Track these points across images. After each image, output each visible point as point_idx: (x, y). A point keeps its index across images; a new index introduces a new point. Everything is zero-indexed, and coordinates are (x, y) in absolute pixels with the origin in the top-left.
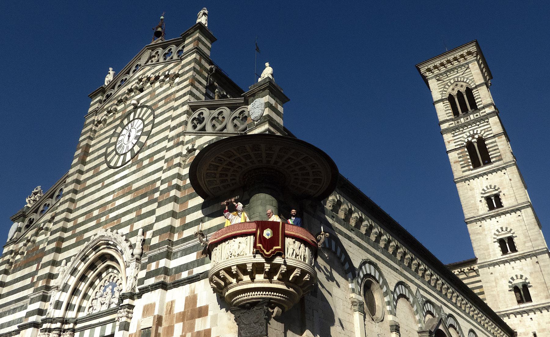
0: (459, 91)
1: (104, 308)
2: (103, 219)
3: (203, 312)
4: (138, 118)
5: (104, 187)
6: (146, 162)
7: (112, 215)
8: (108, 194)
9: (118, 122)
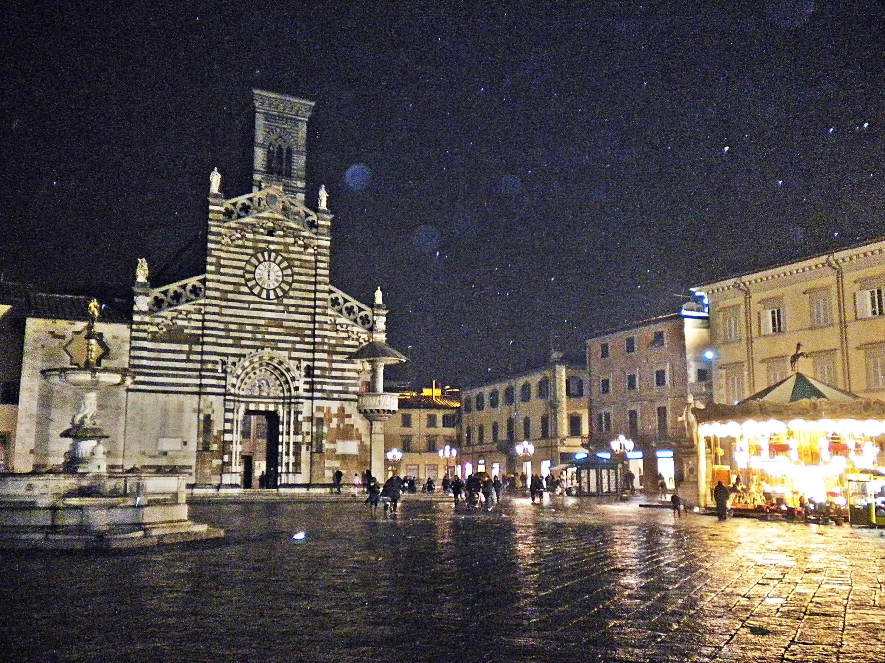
0: (280, 146)
1: (264, 394)
2: (259, 336)
3: (349, 416)
4: (274, 262)
6: (292, 309)
7: (267, 337)
8: (259, 318)
9: (251, 252)
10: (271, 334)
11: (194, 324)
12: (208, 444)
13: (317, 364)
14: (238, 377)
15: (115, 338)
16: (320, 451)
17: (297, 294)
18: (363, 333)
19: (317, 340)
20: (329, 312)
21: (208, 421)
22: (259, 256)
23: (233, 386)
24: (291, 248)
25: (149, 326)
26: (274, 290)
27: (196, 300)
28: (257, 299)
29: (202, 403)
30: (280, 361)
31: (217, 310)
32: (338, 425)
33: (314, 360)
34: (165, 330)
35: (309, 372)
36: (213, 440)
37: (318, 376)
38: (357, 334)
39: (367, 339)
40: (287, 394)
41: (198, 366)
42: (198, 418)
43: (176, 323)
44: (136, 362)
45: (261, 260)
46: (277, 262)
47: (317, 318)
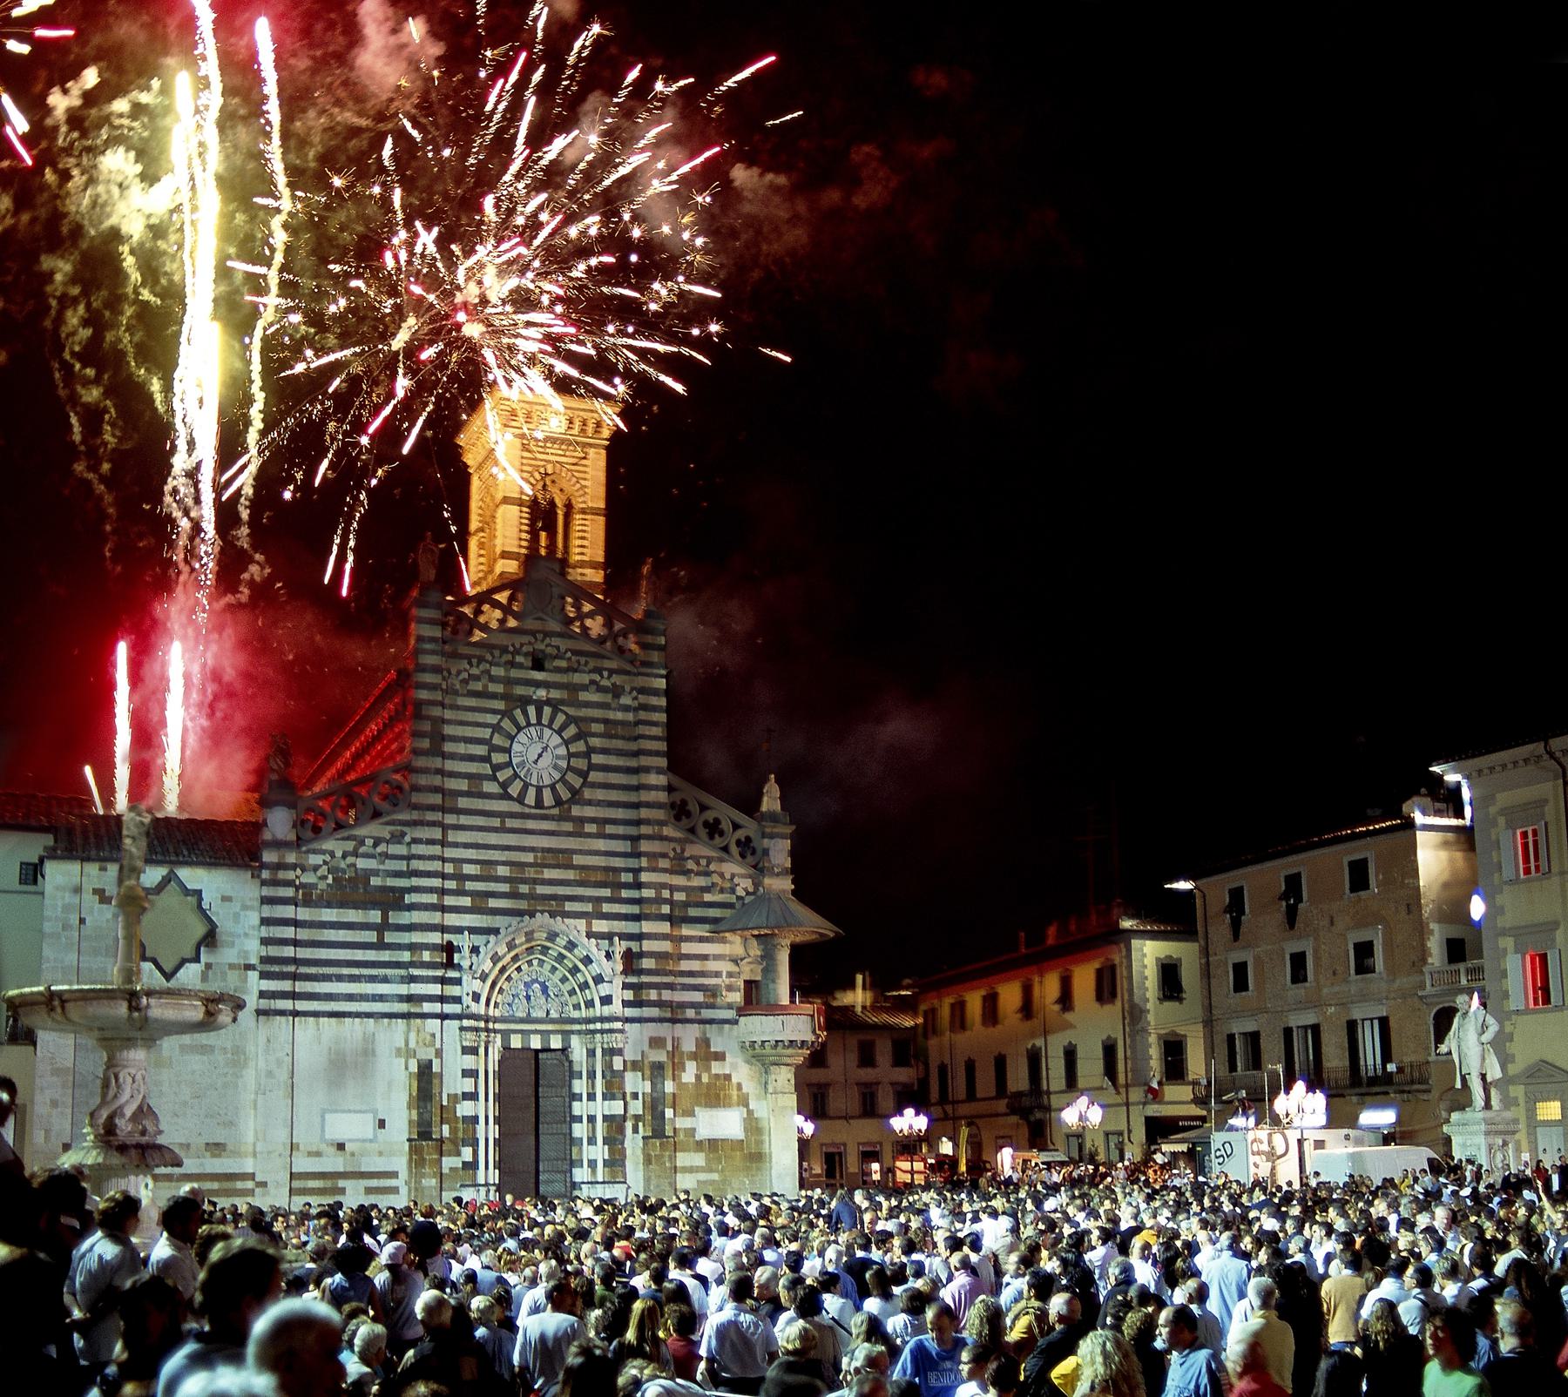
1: (541, 1014)
2: (524, 889)
4: (550, 726)
5: (502, 829)
7: (541, 890)
9: (500, 705)
10: (551, 882)
11: (391, 865)
12: (430, 1125)
13: (647, 945)
14: (484, 977)
15: (226, 899)
16: (658, 1133)
17: (600, 794)
18: (743, 876)
19: (647, 893)
20: (667, 831)
21: (426, 1078)
22: (518, 713)
23: (476, 997)
24: (584, 696)
25: (299, 871)
26: (553, 787)
27: (394, 812)
28: (516, 807)
29: (413, 1036)
30: (570, 942)
31: (437, 833)
32: (698, 1077)
33: (639, 937)
34: (330, 881)
35: (630, 959)
36: (436, 1119)
37: (649, 972)
38: (732, 879)
39: (751, 890)
40: (584, 1013)
41: (406, 956)
42: (407, 1068)
43: (354, 865)
44: (274, 951)
45: (523, 723)
46: (556, 726)
47: (645, 846)
